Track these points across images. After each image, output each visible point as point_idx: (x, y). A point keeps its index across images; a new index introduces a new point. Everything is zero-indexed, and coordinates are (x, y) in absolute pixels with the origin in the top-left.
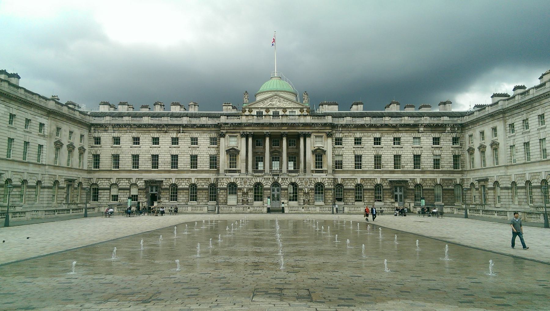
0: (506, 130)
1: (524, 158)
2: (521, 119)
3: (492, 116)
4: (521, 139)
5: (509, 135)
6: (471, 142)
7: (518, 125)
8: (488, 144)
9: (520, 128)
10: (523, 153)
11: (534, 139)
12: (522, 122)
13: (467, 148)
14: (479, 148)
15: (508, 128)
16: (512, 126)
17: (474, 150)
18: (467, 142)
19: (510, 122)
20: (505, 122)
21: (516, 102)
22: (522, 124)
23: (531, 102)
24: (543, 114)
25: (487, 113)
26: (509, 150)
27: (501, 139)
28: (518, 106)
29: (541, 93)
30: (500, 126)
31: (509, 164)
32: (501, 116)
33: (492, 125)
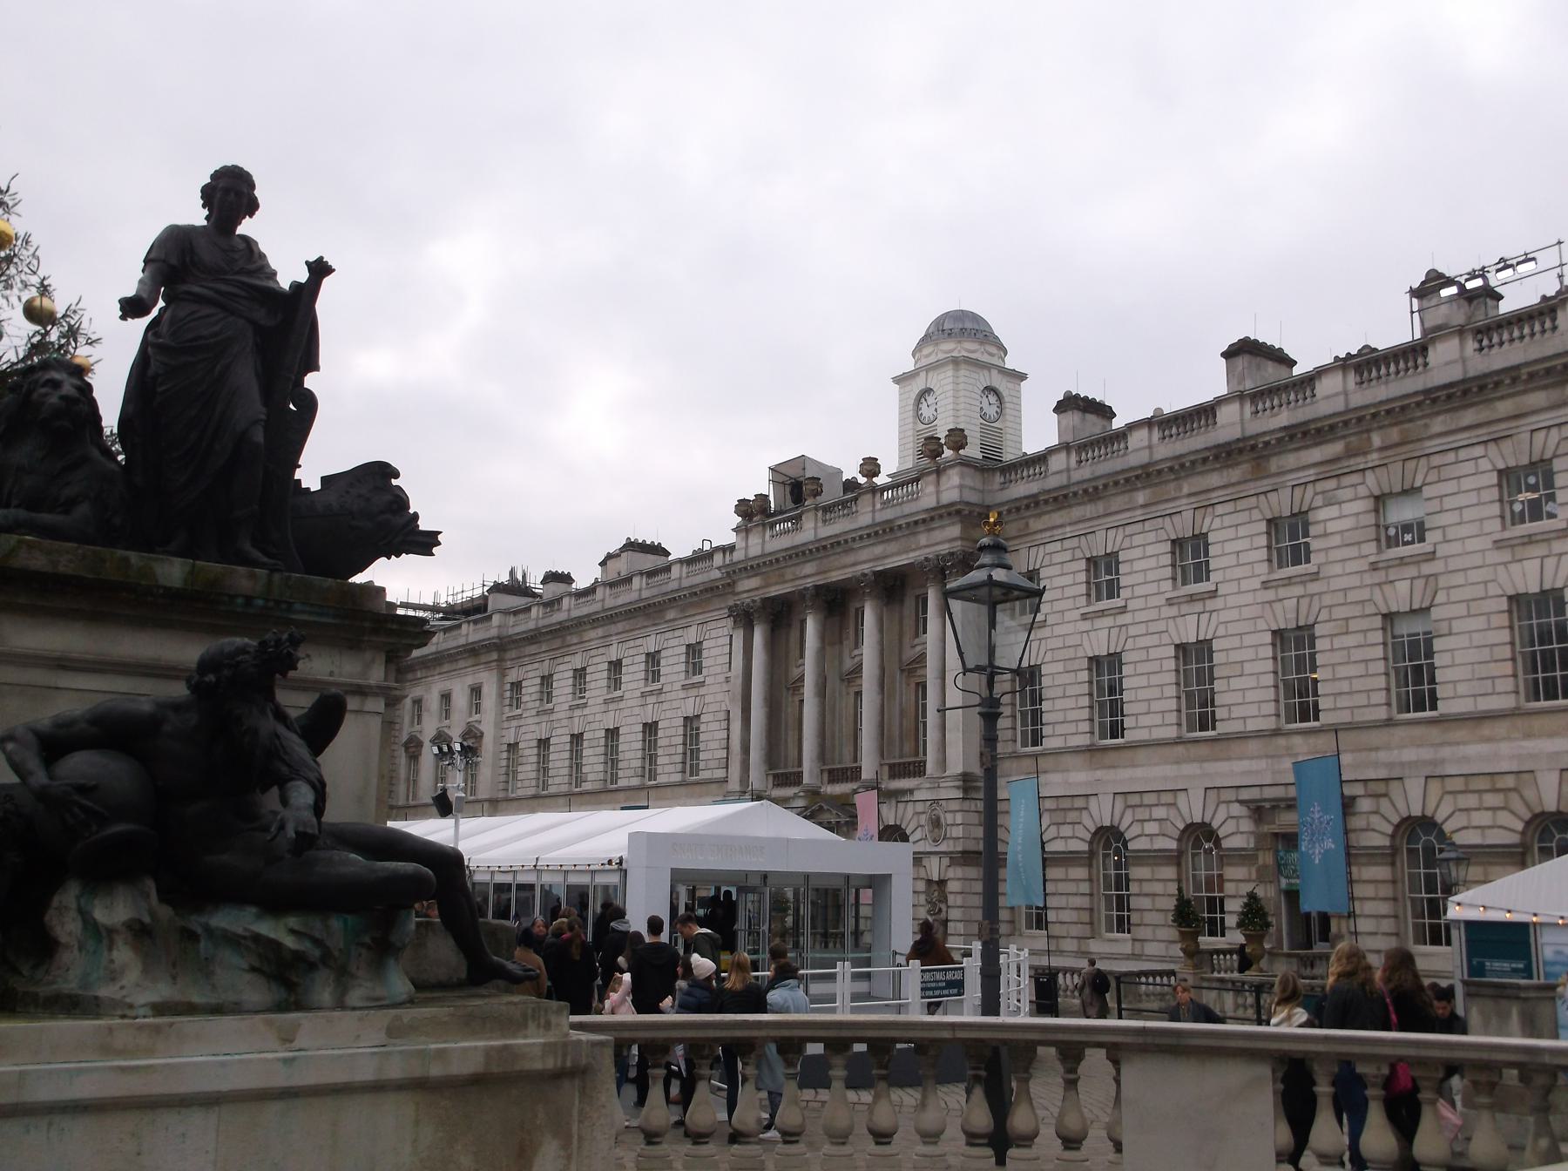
0: (501, 696)
1: (534, 783)
2: (538, 673)
3: (473, 652)
4: (533, 728)
5: (508, 712)
6: (418, 717)
7: (531, 689)
8: (455, 733)
9: (535, 697)
10: (534, 767)
11: (559, 731)
12: (538, 681)
13: (405, 738)
14: (433, 742)
15: (508, 694)
16: (517, 686)
17: (420, 744)
18: (407, 719)
19: (513, 676)
20: (502, 674)
21: (531, 625)
22: (537, 688)
23: (561, 632)
24: (584, 669)
25: (462, 641)
26: (505, 755)
27: (487, 725)
28: (534, 637)
29: (585, 610)
30: (489, 681)
31: (501, 795)
32: (495, 656)
33: (470, 680)
